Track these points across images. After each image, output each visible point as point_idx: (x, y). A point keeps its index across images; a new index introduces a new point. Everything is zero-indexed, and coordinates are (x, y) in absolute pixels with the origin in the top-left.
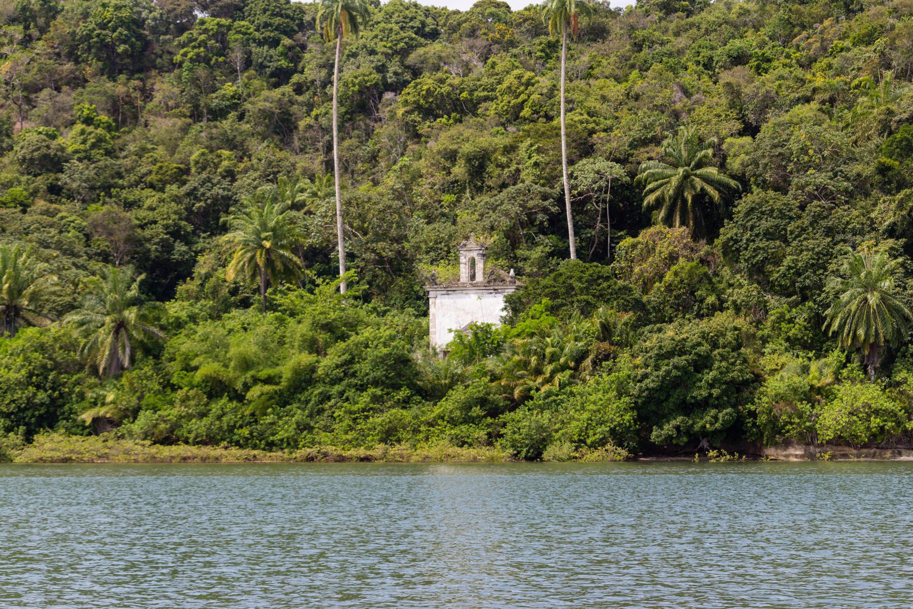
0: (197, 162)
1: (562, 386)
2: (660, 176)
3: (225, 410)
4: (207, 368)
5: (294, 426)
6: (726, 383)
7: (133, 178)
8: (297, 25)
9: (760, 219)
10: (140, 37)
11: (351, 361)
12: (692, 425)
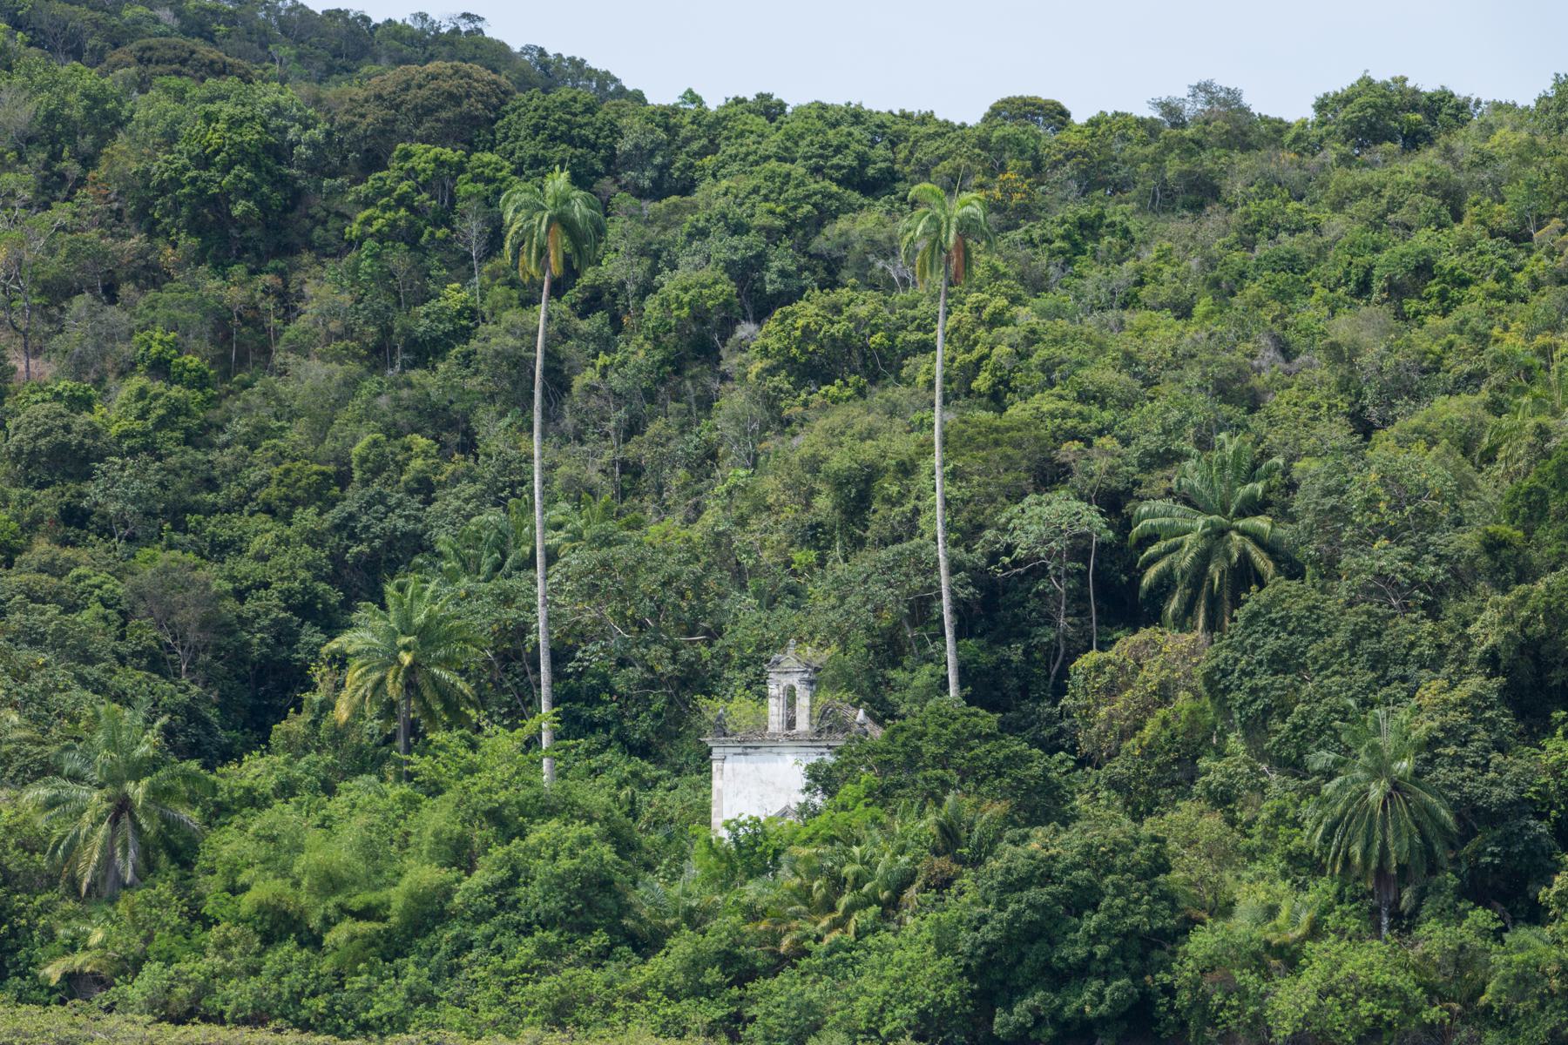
0: (363, 460)
4: (263, 889)
7: (234, 491)
8: (603, 160)
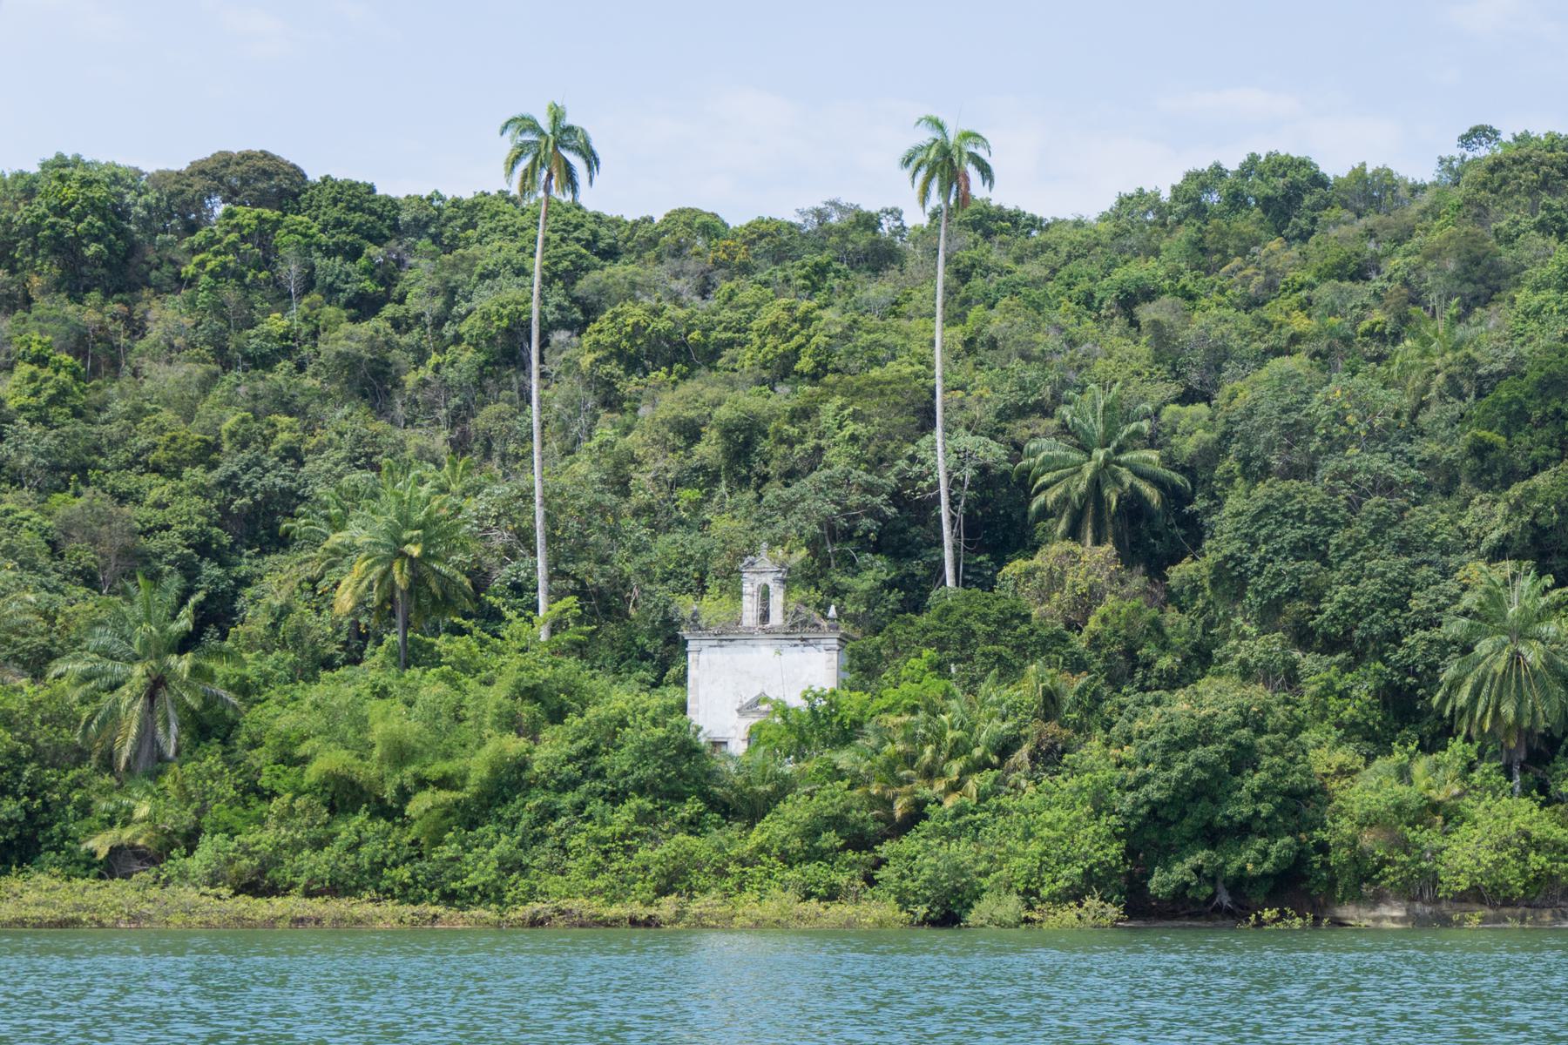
0: (232, 434)
1: (983, 797)
2: (1058, 468)
3: (364, 835)
4: (328, 760)
5: (496, 864)
6: (1281, 793)
7: (122, 455)
8: (389, 227)
9: (1280, 524)
10: (122, 233)
11: (591, 752)
12: (1223, 866)
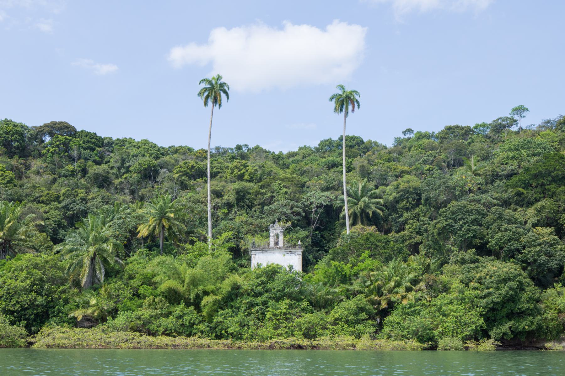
11: (263, 283)
